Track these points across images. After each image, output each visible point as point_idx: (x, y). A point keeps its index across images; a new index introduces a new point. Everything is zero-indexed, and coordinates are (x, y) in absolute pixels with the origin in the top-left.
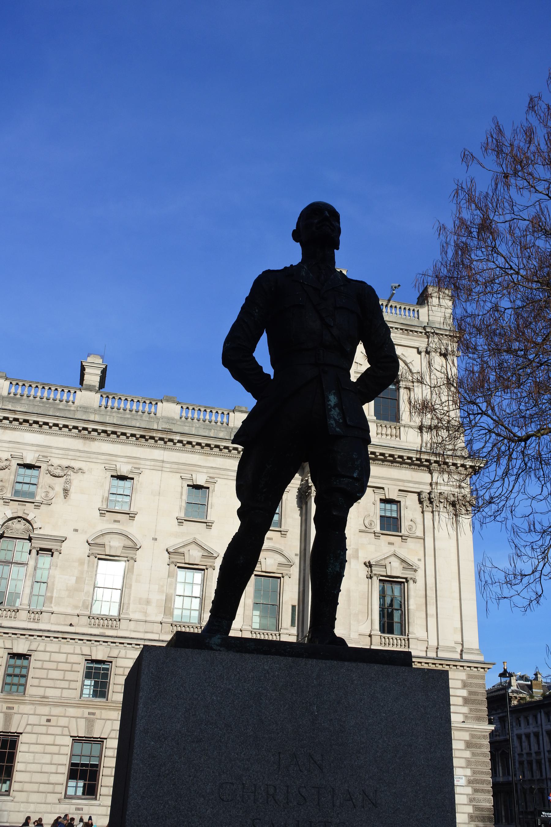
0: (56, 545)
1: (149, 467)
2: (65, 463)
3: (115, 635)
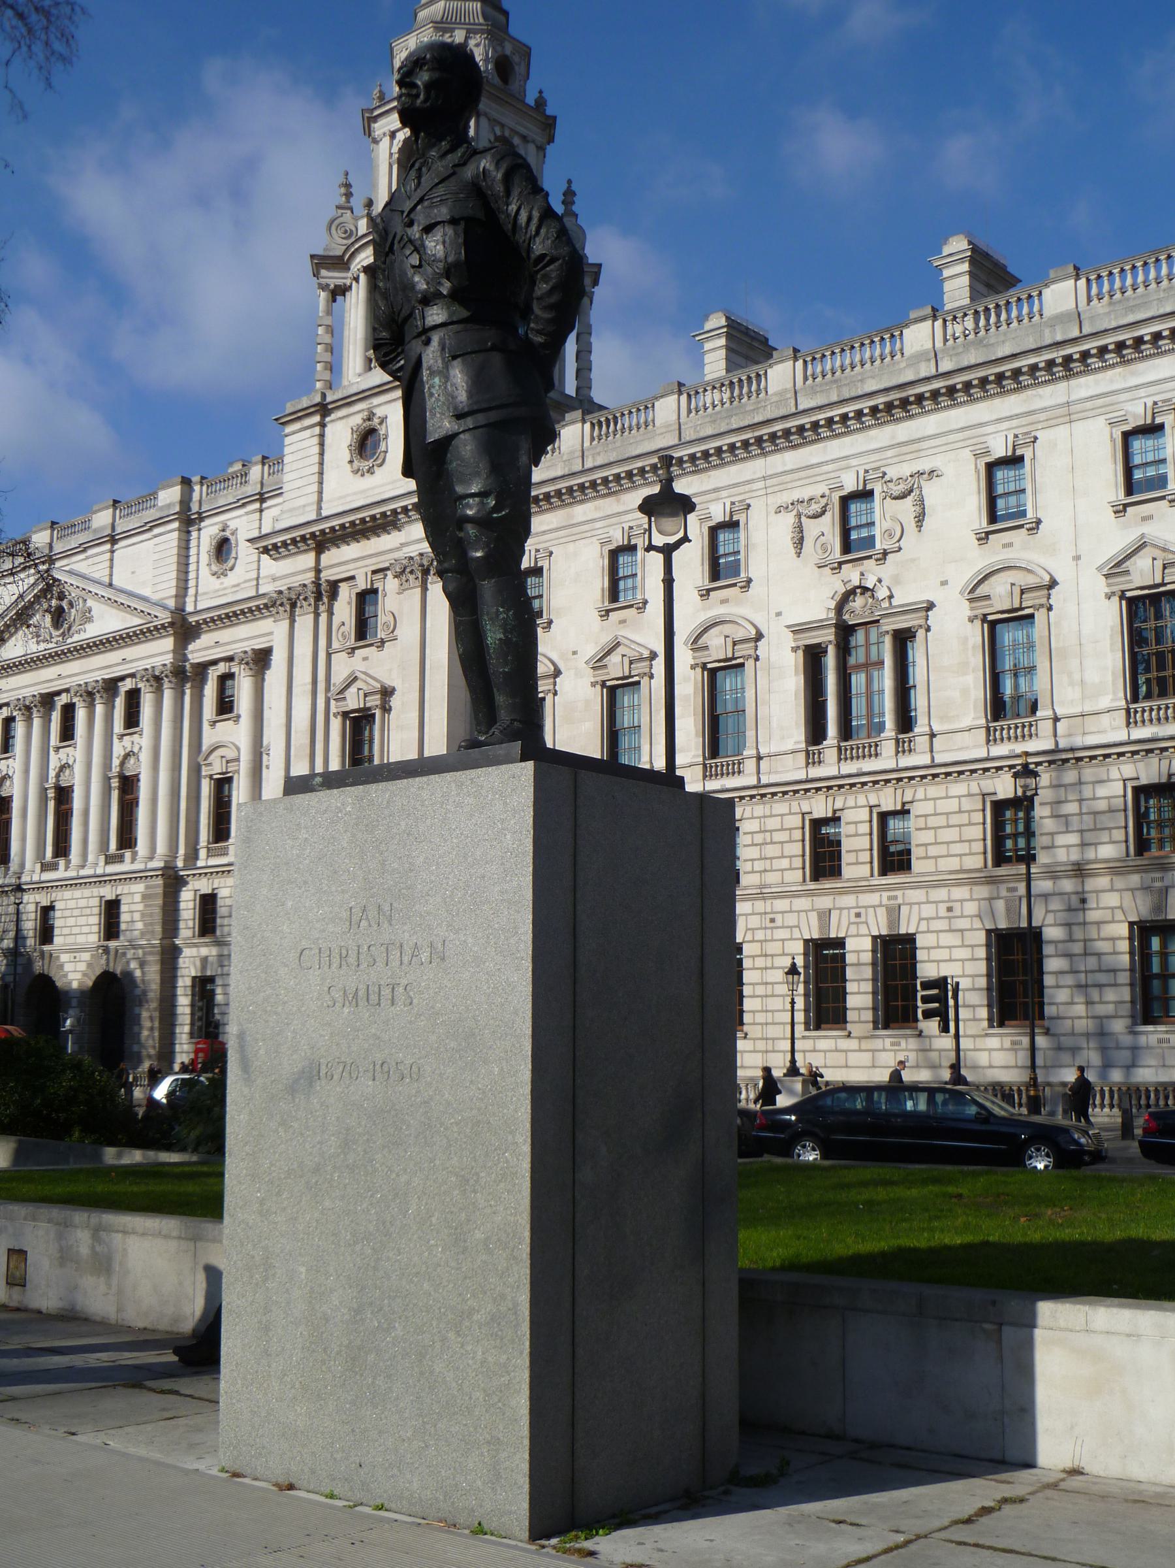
0: (912, 619)
1: (1045, 424)
2: (906, 469)
3: (854, 771)
